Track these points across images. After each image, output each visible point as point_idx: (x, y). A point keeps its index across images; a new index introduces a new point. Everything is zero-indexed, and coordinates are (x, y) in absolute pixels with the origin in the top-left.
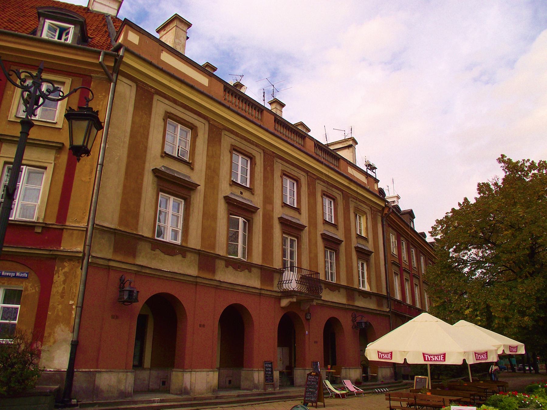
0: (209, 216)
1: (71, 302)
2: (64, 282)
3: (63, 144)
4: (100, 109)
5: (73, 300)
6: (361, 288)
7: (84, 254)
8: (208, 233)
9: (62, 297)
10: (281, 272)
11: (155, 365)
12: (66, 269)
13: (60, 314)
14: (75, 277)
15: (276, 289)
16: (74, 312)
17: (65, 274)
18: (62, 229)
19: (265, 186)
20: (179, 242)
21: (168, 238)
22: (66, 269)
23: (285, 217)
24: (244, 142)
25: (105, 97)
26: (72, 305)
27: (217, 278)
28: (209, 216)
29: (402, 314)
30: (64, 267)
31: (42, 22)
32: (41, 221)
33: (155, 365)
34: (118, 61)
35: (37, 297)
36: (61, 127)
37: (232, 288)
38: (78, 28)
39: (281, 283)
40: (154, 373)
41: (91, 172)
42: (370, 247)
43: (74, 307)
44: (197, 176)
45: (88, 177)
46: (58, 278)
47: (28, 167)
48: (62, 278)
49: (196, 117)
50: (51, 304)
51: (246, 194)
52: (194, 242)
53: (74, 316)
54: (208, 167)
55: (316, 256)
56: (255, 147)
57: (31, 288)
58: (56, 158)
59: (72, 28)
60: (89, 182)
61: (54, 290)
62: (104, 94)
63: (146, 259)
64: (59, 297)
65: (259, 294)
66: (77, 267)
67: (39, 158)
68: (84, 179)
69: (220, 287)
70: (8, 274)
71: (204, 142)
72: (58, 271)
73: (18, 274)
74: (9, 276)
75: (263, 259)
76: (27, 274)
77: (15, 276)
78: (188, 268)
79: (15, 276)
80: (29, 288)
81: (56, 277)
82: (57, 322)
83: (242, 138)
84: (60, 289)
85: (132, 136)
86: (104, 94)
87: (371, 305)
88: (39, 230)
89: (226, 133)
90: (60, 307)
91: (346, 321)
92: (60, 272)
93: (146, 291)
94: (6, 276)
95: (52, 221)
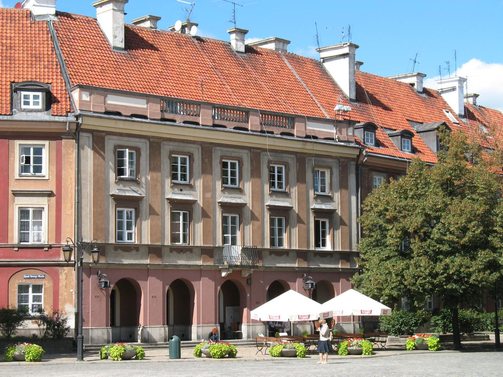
1: (71, 290)
2: (66, 279)
3: (52, 191)
4: (71, 161)
5: (72, 289)
7: (75, 262)
9: (66, 288)
11: (122, 324)
12: (66, 271)
13: (66, 297)
14: (72, 276)
16: (74, 296)
17: (66, 274)
18: (60, 247)
22: (66, 271)
24: (181, 144)
25: (73, 151)
26: (72, 292)
29: (277, 289)
30: (64, 270)
31: (20, 94)
32: (47, 243)
33: (122, 324)
35: (52, 288)
36: (48, 178)
38: (44, 93)
40: (124, 329)
41: (72, 208)
43: (73, 293)
45: (70, 211)
46: (62, 277)
47: (33, 209)
48: (64, 277)
49: (137, 140)
50: (60, 292)
53: (74, 298)
56: (192, 145)
58: (48, 201)
59: (40, 94)
60: (71, 215)
61: (61, 285)
62: (72, 149)
64: (64, 288)
66: (72, 270)
67: (38, 202)
68: (68, 213)
70: (33, 277)
71: (146, 158)
72: (61, 273)
73: (39, 276)
74: (34, 278)
76: (44, 275)
77: (38, 278)
79: (38, 278)
80: (47, 284)
81: (60, 276)
82: (65, 302)
83: (179, 142)
84: (64, 283)
85: (94, 175)
86: (72, 149)
88: (47, 249)
89: (165, 143)
90: (65, 293)
92: (63, 273)
94: (33, 278)
95: (52, 242)
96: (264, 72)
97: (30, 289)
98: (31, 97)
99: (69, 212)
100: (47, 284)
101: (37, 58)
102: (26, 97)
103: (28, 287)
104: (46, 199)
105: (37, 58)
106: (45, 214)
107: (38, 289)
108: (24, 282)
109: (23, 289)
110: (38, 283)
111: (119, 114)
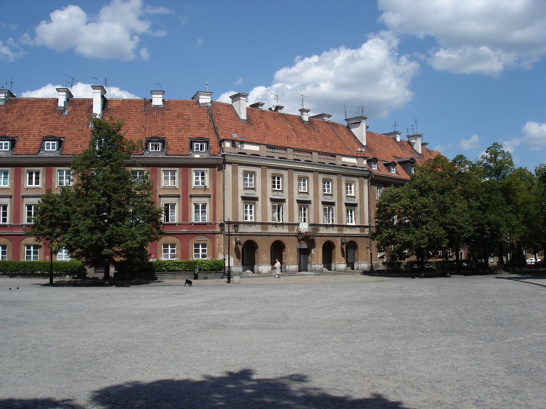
0: (264, 208)
6: (349, 224)
8: (264, 214)
10: (298, 225)
15: (296, 232)
19: (289, 187)
20: (253, 220)
21: (249, 220)
23: (300, 199)
27: (269, 231)
28: (264, 208)
34: (224, 160)
37: (275, 235)
39: (298, 229)
42: (357, 201)
44: (258, 194)
51: (280, 193)
52: (259, 220)
54: (262, 188)
55: (318, 213)
57: (209, 243)
63: (242, 229)
65: (288, 235)
69: (270, 235)
75: (289, 220)
78: (257, 229)
87: (357, 232)
91: (338, 243)
93: (243, 240)
95: (212, 221)
96: (318, 131)
97: (200, 246)
98: (51, 148)
99: (219, 205)
100: (209, 243)
101: (202, 125)
102: (48, 144)
103: (199, 245)
104: (208, 199)
105: (202, 125)
106: (207, 207)
107: (204, 245)
108: (197, 242)
109: (197, 245)
110: (204, 242)
111: (245, 154)
